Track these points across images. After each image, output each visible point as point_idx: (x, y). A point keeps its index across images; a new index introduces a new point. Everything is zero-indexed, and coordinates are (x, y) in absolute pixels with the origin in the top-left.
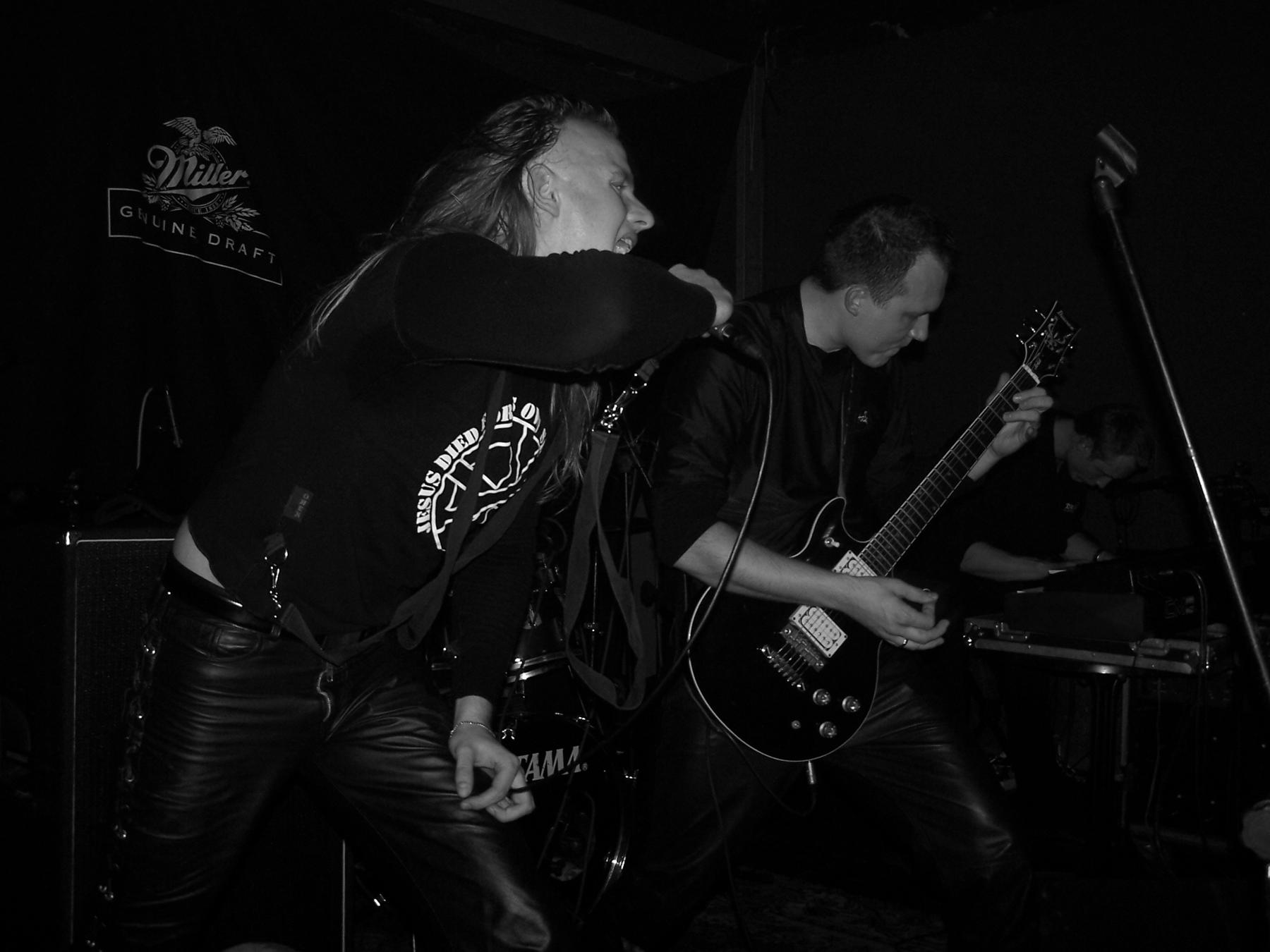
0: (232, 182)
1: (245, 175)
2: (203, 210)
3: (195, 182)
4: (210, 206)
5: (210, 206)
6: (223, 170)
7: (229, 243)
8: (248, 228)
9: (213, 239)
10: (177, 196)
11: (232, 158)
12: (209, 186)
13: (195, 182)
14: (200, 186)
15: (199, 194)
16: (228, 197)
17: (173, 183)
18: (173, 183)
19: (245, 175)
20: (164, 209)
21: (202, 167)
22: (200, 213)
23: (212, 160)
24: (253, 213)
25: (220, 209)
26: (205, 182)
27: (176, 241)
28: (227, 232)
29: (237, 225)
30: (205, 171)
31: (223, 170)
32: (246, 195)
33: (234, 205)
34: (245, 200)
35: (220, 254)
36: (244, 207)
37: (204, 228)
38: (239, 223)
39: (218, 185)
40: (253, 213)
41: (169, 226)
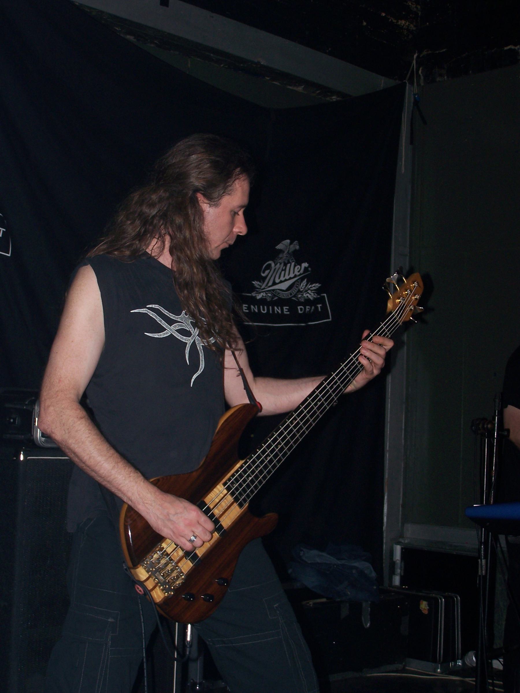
0: (302, 271)
5: (294, 291)
6: (295, 266)
10: (273, 290)
12: (290, 278)
13: (282, 279)
14: (286, 280)
15: (284, 286)
16: (302, 282)
20: (269, 299)
22: (290, 296)
23: (289, 262)
24: (318, 285)
25: (299, 291)
26: (287, 277)
27: (281, 318)
28: (308, 302)
29: (311, 295)
30: (285, 270)
31: (295, 266)
32: (309, 277)
33: (306, 285)
34: (311, 280)
35: (306, 317)
37: (292, 303)
39: (295, 276)
40: (318, 285)
41: (273, 309)
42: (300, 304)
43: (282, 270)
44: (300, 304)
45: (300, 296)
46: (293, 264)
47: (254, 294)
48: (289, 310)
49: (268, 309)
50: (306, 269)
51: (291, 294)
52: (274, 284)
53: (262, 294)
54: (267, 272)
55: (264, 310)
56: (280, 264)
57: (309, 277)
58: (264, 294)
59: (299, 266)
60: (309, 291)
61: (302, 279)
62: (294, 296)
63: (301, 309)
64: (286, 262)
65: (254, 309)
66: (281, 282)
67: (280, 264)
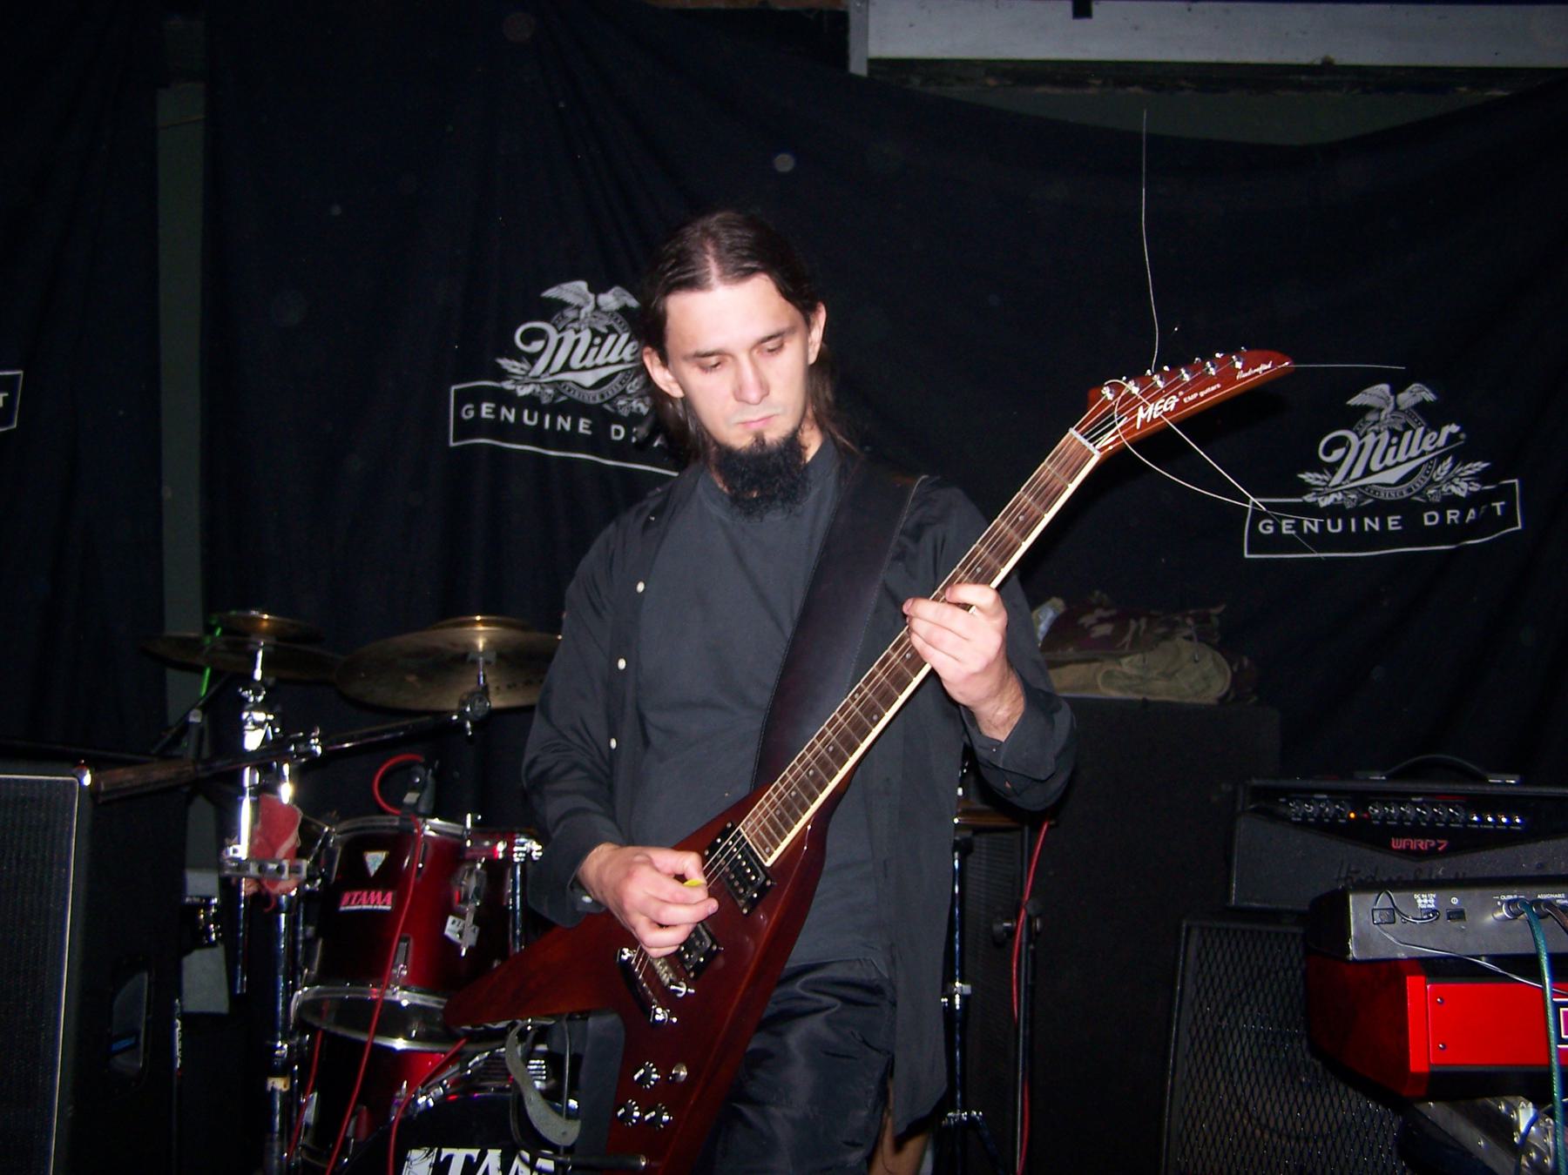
0: (1441, 442)
1: (1454, 428)
2: (1409, 490)
3: (1389, 461)
4: (1417, 482)
5: (1417, 482)
6: (1425, 434)
7: (1452, 515)
8: (1476, 487)
9: (1429, 520)
10: (1363, 487)
11: (1431, 416)
12: (1410, 459)
16: (1440, 463)
17: (1357, 472)
18: (1357, 472)
19: (1454, 428)
21: (1395, 440)
22: (1406, 495)
24: (1480, 466)
25: (1431, 482)
26: (1401, 457)
28: (1451, 501)
29: (1461, 489)
31: (1425, 434)
32: (1459, 453)
35: (1443, 532)
36: (1464, 464)
37: (1409, 509)
38: (1464, 485)
40: (1480, 466)
42: (1429, 506)
43: (1390, 445)
44: (1429, 506)
45: (1431, 492)
46: (1420, 431)
47: (1309, 498)
48: (1401, 522)
49: (1347, 525)
50: (1452, 438)
51: (1409, 490)
52: (1367, 472)
53: (1333, 496)
54: (1337, 454)
55: (1335, 526)
56: (1377, 433)
57: (1459, 453)
58: (1340, 496)
59: (1435, 434)
60: (1456, 481)
61: (1441, 459)
62: (1418, 494)
63: (1431, 518)
64: (1399, 428)
65: (1311, 525)
66: (1386, 468)
67: (1377, 433)
